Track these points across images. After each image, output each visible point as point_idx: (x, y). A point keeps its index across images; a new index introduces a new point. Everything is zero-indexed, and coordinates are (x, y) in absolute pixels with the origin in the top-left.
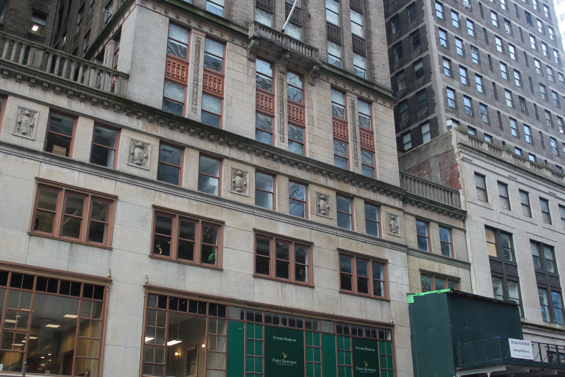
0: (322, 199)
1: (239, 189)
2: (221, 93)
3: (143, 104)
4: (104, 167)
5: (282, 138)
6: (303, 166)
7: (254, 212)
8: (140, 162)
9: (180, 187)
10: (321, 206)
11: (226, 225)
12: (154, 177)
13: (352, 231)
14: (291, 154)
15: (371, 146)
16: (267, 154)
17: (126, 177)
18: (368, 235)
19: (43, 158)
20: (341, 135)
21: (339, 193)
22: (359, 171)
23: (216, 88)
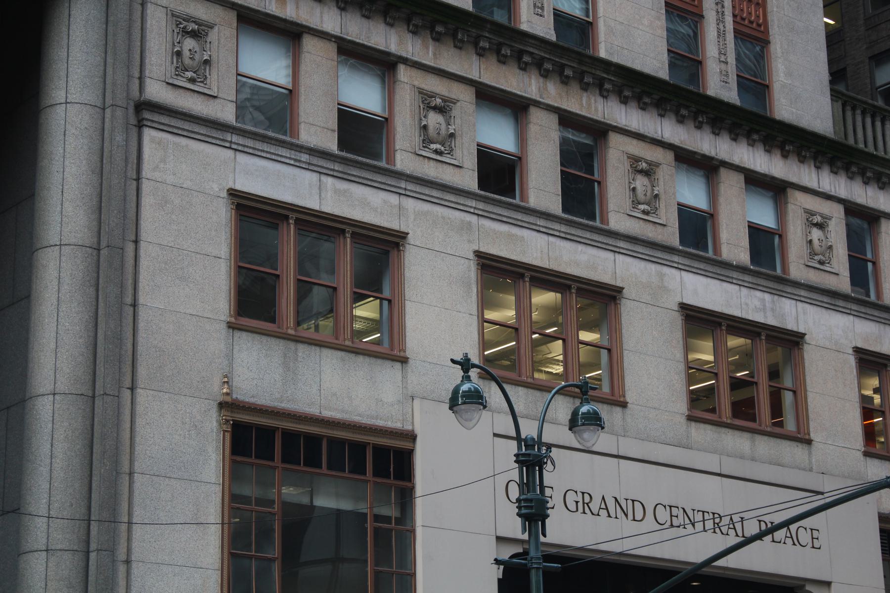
0: (641, 172)
1: (438, 146)
2: (762, 28)
3: (726, 100)
4: (701, 253)
5: (723, 73)
6: (490, 49)
7: (405, 189)
8: (443, 148)
9: (392, 168)
10: (816, 242)
11: (625, 296)
12: (674, 240)
13: (714, 257)
14: (542, 42)
15: (759, 25)
16: (526, 58)
17: (628, 244)
18: (757, 269)
19: (829, 301)
20: (751, 22)
21: (852, 210)
22: (731, 95)
23: (745, 15)
